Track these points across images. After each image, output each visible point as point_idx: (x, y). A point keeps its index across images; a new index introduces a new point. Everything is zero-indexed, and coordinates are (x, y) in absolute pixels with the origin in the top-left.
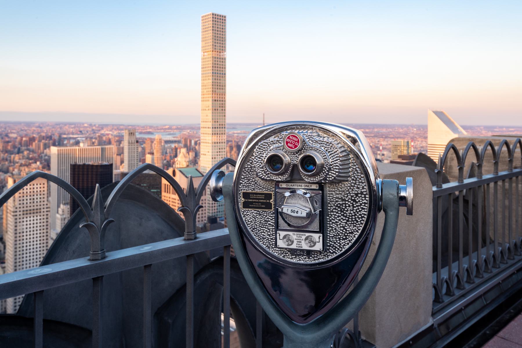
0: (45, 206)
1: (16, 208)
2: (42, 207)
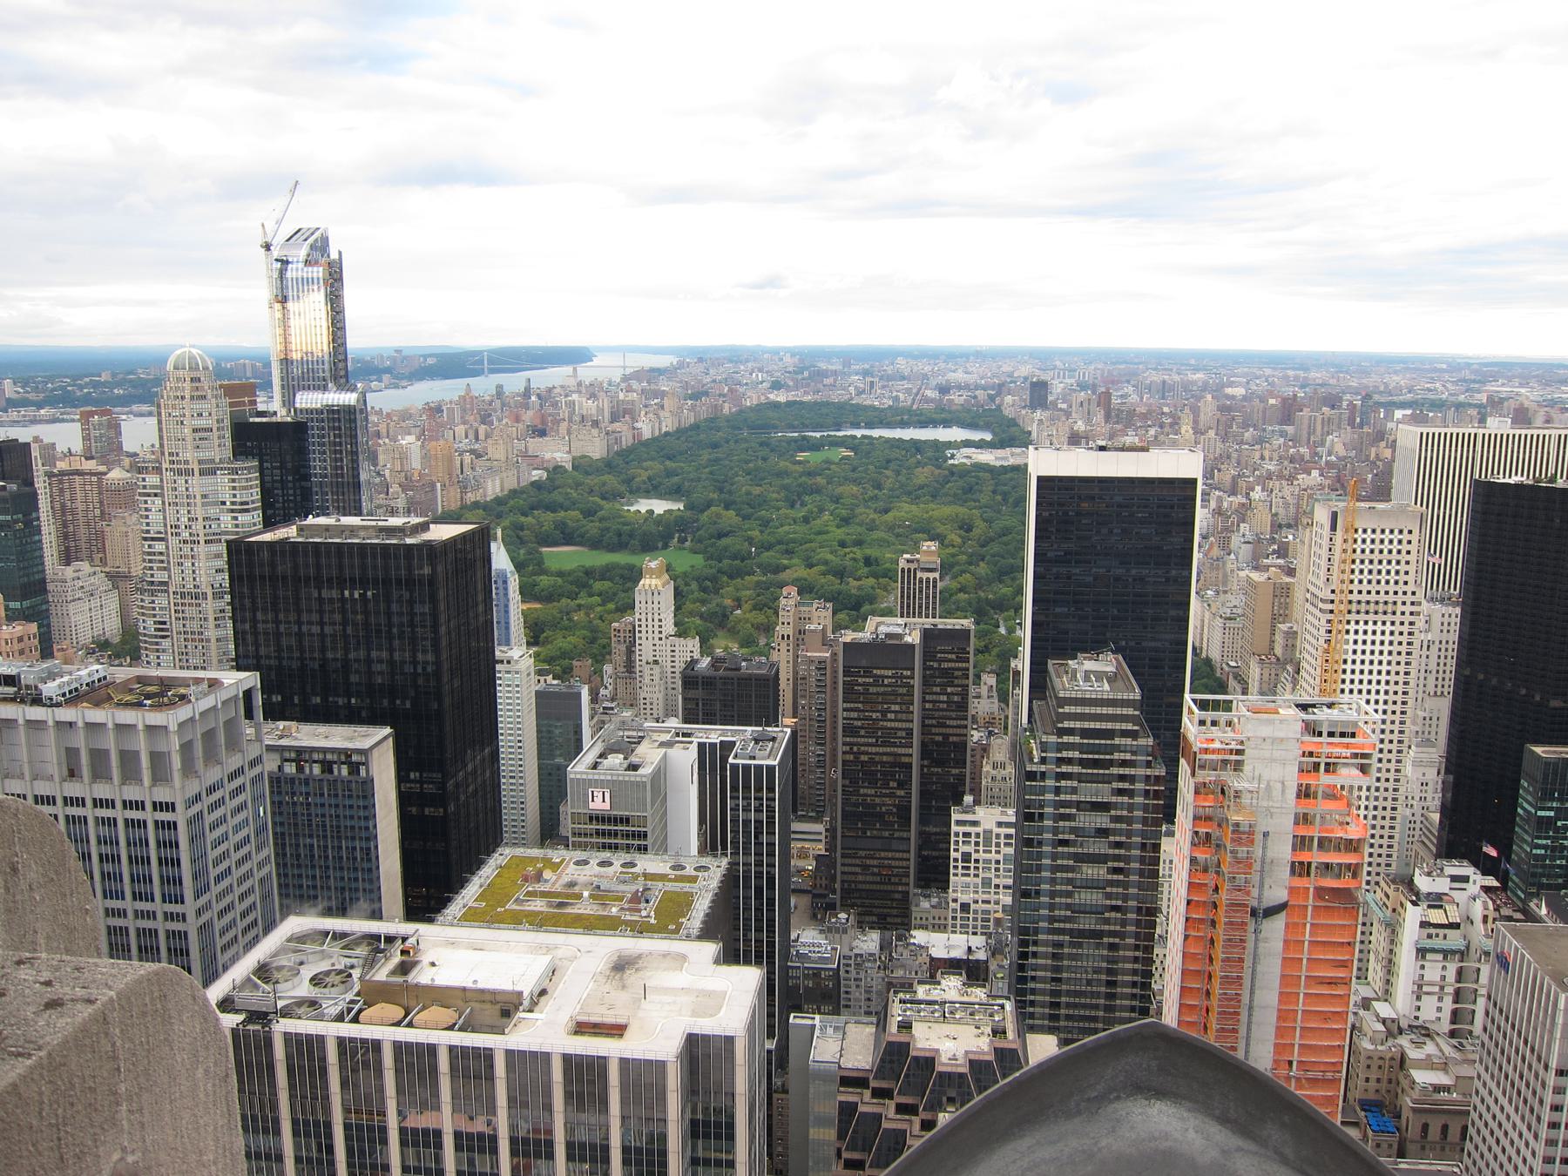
0: (1409, 598)
1: (1333, 592)
2: (1400, 598)
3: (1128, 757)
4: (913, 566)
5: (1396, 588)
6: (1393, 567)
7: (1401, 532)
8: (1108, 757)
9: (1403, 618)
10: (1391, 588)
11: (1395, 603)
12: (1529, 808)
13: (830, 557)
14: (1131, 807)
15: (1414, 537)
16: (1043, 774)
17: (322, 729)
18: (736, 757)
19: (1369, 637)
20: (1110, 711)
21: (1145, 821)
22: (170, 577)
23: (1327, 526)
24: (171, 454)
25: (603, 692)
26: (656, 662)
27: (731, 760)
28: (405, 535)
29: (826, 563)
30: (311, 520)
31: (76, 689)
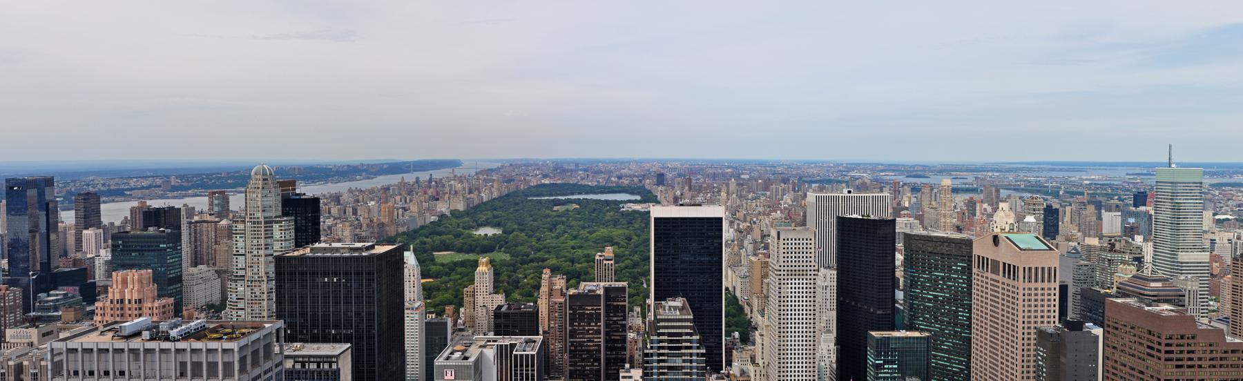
0: (812, 268)
1: (780, 266)
2: (809, 268)
3: (689, 344)
4: (602, 258)
5: (807, 264)
6: (805, 255)
7: (807, 240)
8: (680, 345)
9: (810, 277)
10: (805, 264)
11: (807, 270)
12: (872, 360)
13: (567, 254)
14: (691, 368)
15: (813, 242)
16: (652, 354)
17: (315, 346)
18: (516, 351)
19: (797, 286)
20: (680, 324)
21: (698, 374)
22: (246, 273)
23: (776, 238)
24: (250, 215)
25: (459, 321)
26: (484, 306)
27: (514, 353)
28: (363, 251)
29: (565, 257)
30: (317, 245)
31: (188, 332)
